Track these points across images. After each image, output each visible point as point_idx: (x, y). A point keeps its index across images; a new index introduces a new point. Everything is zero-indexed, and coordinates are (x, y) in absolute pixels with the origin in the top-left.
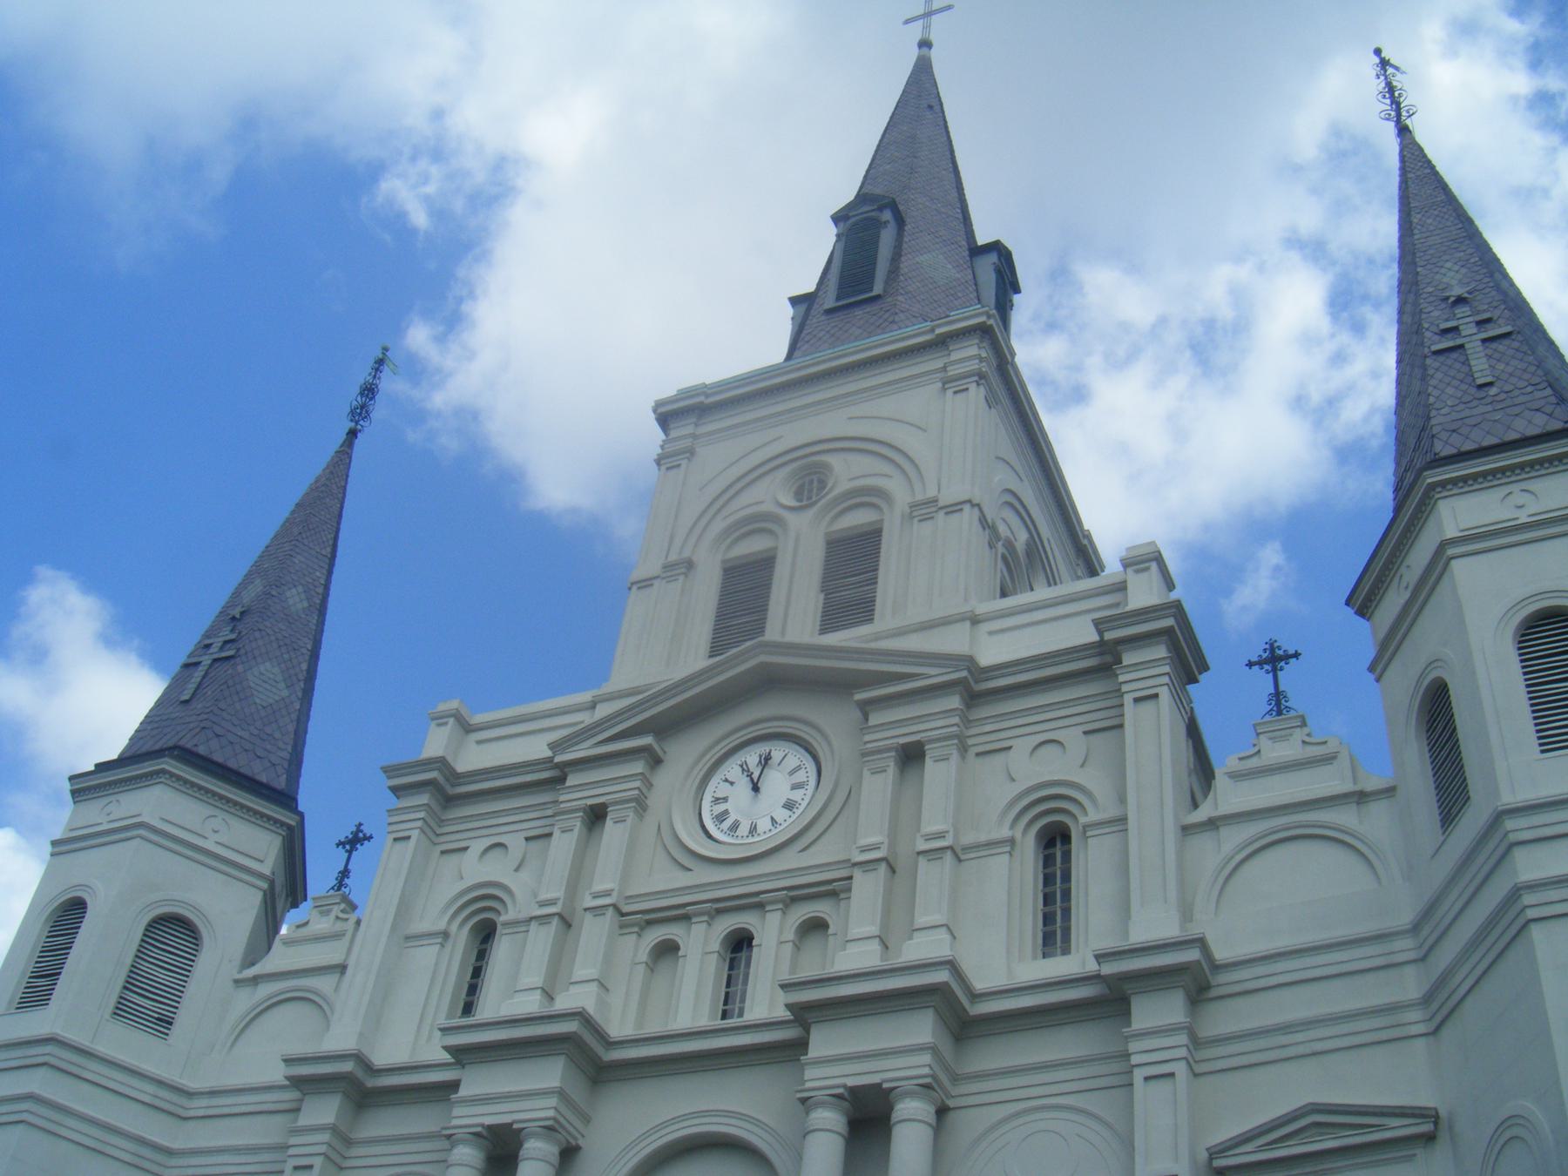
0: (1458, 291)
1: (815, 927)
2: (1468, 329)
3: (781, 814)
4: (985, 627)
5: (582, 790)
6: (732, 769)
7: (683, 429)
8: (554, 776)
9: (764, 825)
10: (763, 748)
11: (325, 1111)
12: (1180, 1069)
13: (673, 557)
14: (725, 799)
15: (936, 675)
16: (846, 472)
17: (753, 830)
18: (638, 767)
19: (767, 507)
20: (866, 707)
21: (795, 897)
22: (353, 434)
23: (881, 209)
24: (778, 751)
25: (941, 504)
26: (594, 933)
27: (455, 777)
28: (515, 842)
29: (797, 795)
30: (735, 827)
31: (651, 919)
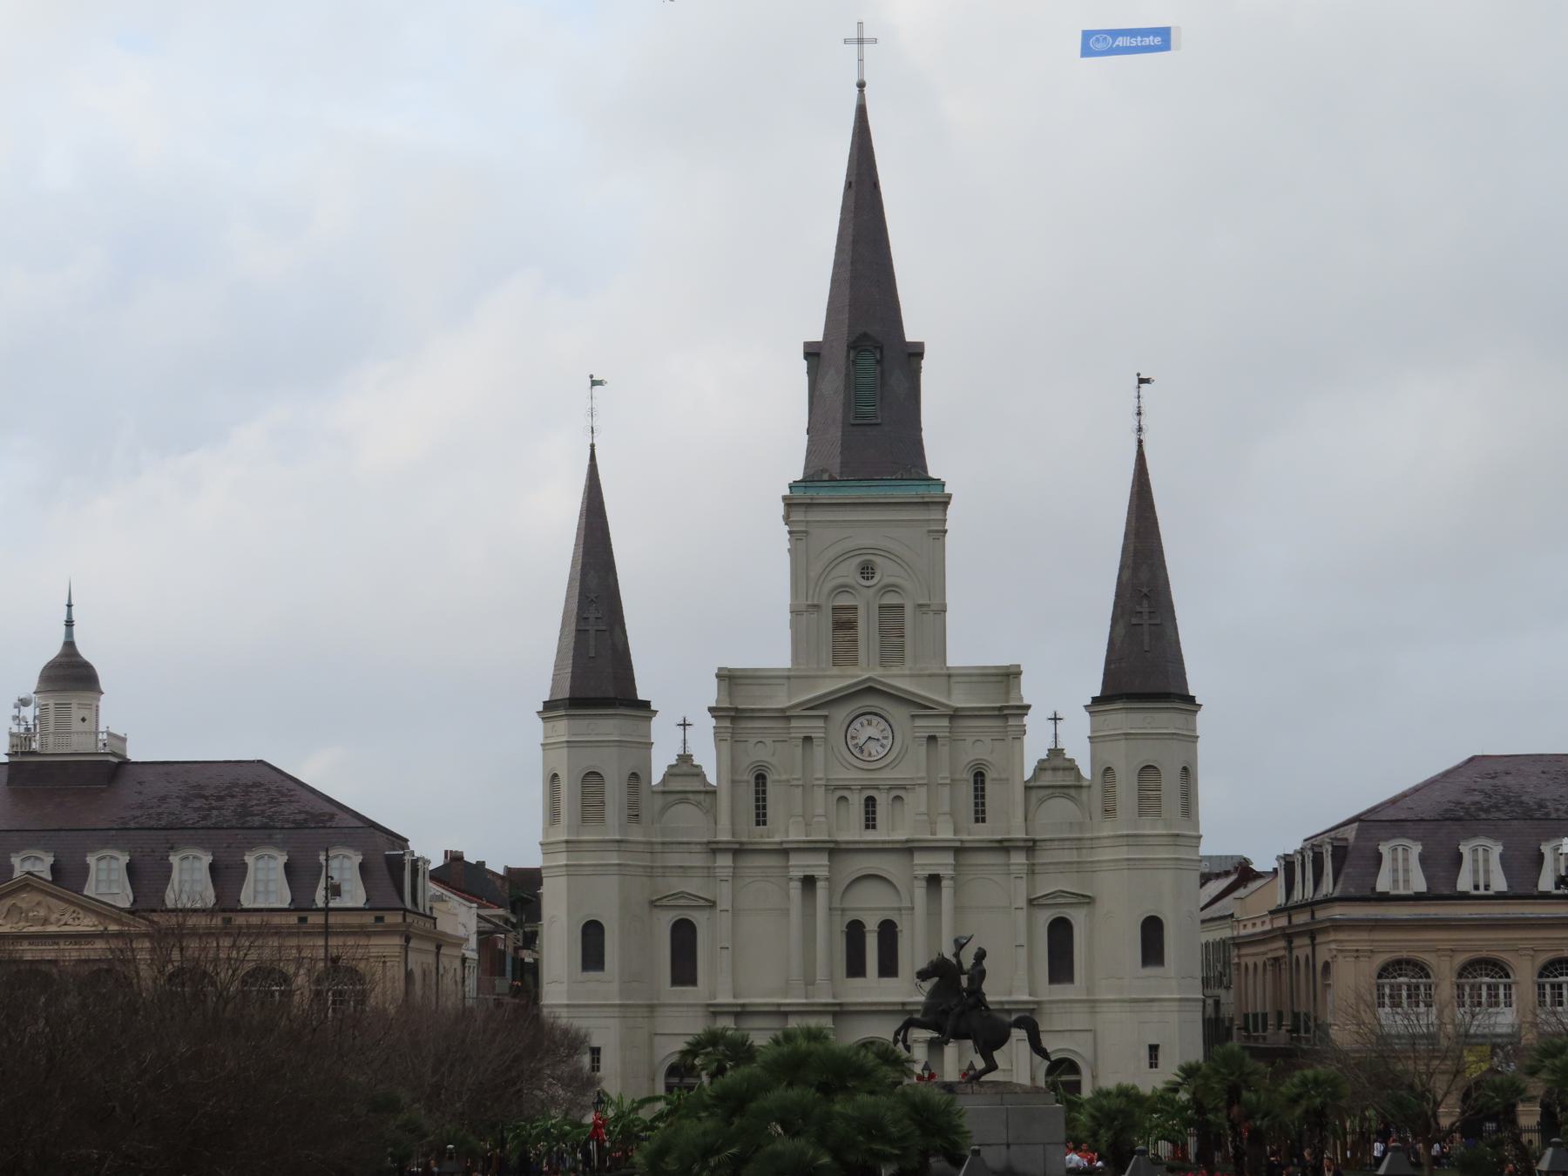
0: (1145, 590)
1: (898, 798)
2: (1146, 617)
3: (880, 749)
4: (953, 679)
5: (800, 727)
6: (856, 724)
7: (798, 516)
8: (784, 716)
9: (874, 752)
10: (868, 717)
11: (725, 861)
12: (1025, 876)
13: (810, 602)
14: (856, 737)
15: (942, 710)
16: (886, 571)
17: (870, 755)
18: (821, 723)
19: (849, 581)
20: (913, 717)
21: (892, 788)
22: (592, 446)
23: (876, 348)
24: (875, 720)
25: (932, 608)
26: (820, 794)
27: (737, 710)
28: (768, 741)
29: (885, 742)
30: (862, 751)
31: (837, 788)
